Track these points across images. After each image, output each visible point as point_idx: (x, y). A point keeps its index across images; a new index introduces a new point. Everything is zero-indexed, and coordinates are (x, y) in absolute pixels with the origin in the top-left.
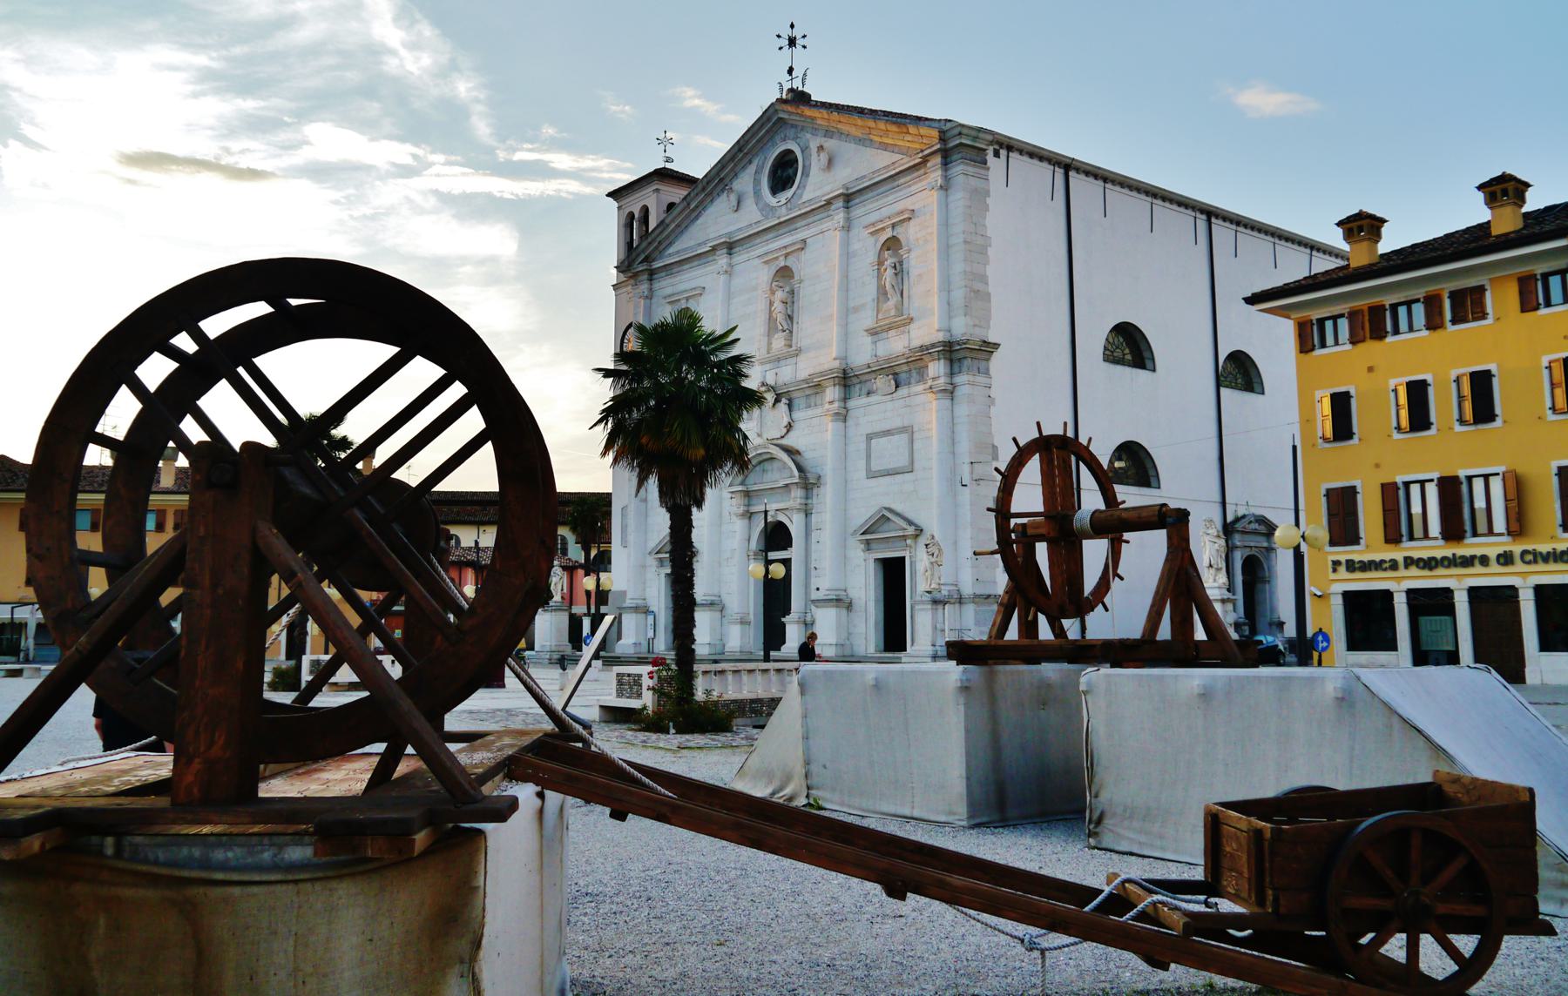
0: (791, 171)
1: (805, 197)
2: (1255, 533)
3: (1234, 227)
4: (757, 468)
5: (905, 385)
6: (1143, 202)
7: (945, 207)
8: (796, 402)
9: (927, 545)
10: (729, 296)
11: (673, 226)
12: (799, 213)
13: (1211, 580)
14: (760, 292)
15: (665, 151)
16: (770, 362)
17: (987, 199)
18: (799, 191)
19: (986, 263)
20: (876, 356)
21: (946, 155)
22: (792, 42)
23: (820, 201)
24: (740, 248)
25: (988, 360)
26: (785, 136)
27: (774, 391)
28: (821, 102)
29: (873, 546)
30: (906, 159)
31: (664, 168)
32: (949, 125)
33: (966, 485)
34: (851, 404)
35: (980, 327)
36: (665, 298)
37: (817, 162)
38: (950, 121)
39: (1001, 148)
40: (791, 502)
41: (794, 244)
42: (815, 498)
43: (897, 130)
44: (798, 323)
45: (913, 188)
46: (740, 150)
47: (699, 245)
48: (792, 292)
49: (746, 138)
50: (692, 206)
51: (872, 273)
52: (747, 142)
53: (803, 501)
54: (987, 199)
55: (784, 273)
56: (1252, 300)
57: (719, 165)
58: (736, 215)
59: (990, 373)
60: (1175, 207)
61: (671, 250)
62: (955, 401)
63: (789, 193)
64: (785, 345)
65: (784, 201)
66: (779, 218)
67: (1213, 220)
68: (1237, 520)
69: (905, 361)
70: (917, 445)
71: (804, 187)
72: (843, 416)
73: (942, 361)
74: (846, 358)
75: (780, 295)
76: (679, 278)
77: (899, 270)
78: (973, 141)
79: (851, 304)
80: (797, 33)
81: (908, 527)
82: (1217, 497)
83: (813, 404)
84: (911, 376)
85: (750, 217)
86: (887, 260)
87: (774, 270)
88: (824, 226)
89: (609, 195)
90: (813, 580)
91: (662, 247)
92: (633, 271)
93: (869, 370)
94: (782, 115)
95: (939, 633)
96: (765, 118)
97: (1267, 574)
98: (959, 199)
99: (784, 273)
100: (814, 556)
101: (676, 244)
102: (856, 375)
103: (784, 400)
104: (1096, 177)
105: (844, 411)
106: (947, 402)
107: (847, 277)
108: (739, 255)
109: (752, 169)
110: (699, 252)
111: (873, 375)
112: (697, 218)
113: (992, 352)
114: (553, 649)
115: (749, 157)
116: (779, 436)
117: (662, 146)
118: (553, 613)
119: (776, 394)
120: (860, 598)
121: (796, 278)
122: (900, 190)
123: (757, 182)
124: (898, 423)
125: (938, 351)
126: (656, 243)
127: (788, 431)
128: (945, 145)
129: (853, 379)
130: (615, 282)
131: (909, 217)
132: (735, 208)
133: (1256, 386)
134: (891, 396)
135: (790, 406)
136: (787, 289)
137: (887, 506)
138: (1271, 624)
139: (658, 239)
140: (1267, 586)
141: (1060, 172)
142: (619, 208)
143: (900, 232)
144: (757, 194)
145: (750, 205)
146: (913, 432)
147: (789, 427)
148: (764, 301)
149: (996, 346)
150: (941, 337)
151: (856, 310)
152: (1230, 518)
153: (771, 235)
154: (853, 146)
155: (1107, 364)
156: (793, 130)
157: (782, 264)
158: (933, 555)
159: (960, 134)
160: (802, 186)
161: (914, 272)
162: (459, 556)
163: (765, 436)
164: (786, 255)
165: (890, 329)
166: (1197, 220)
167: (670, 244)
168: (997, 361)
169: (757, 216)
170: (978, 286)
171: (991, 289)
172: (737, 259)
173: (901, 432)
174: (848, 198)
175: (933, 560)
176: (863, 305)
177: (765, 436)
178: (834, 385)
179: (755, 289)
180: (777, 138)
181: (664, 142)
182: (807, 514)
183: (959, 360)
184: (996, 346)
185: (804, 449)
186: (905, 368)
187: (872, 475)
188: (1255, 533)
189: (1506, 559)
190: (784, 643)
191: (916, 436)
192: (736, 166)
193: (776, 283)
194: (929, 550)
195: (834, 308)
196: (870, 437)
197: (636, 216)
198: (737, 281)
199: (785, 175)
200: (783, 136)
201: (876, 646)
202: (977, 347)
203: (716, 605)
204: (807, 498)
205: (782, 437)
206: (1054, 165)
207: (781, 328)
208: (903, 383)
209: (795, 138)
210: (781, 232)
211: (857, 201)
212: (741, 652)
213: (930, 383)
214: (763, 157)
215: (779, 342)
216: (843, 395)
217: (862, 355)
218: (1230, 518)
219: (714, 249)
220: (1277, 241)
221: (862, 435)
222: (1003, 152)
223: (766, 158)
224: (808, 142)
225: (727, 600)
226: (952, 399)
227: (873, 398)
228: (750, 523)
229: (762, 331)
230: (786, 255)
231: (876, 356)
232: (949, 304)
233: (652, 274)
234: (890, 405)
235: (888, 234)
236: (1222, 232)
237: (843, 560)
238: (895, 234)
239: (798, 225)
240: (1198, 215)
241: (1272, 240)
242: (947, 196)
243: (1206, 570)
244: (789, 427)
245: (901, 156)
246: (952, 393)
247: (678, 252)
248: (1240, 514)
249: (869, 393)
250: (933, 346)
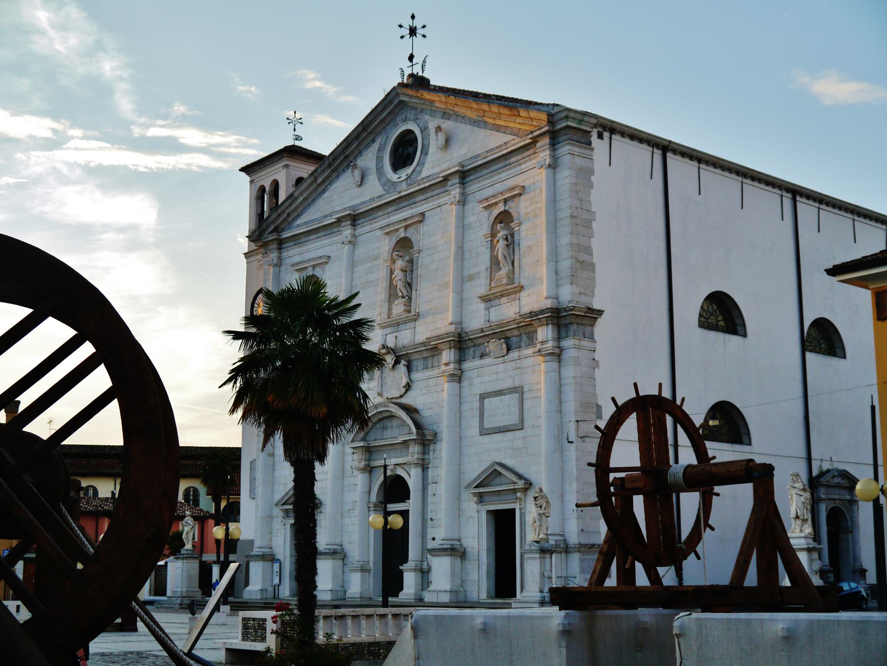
1: (424, 174)
2: (838, 486)
3: (817, 205)
4: (378, 426)
5: (516, 348)
6: (732, 182)
7: (553, 184)
8: (414, 363)
9: (535, 498)
10: (353, 264)
11: (301, 199)
12: (418, 188)
13: (798, 530)
14: (382, 261)
15: (295, 130)
16: (390, 326)
17: (592, 177)
18: (418, 168)
19: (591, 236)
20: (489, 321)
21: (555, 136)
22: (413, 31)
23: (439, 177)
24: (364, 220)
25: (593, 325)
26: (406, 117)
27: (394, 353)
28: (439, 87)
29: (486, 498)
30: (518, 140)
31: (294, 146)
32: (556, 109)
33: (572, 442)
34: (466, 365)
35: (585, 295)
36: (293, 265)
37: (435, 142)
38: (557, 105)
39: (605, 130)
40: (410, 457)
41: (413, 216)
42: (431, 453)
43: (509, 113)
44: (416, 290)
45: (523, 166)
46: (364, 130)
47: (326, 217)
48: (411, 262)
49: (370, 119)
50: (318, 183)
51: (484, 243)
52: (371, 123)
53: (421, 456)
54: (592, 177)
55: (404, 245)
56: (833, 272)
57: (345, 143)
58: (360, 189)
59: (596, 337)
60: (763, 186)
61: (299, 222)
62: (562, 364)
63: (409, 170)
64: (404, 310)
65: (404, 177)
66: (399, 192)
67: (798, 198)
68: (822, 474)
69: (516, 326)
70: (527, 404)
71: (423, 164)
72: (457, 377)
73: (550, 327)
74: (461, 323)
75: (400, 263)
76: (305, 248)
77: (511, 242)
78: (578, 123)
79: (466, 273)
80: (418, 23)
81: (518, 481)
82: (802, 453)
83: (430, 366)
84: (521, 341)
85: (373, 191)
86: (499, 232)
87: (394, 240)
88: (442, 201)
89: (242, 170)
90: (430, 530)
91: (290, 219)
92: (263, 241)
93: (483, 334)
94: (403, 98)
95: (546, 580)
96: (387, 101)
97: (850, 525)
98: (566, 177)
99: (404, 245)
100: (430, 508)
101: (304, 216)
102: (471, 339)
103: (403, 362)
104: (691, 158)
105: (458, 373)
106: (555, 365)
107: (462, 248)
108: (363, 227)
109: (375, 146)
110: (325, 223)
111: (487, 339)
112: (324, 191)
113: (597, 318)
114: (184, 594)
115: (372, 136)
116: (398, 396)
117: (292, 125)
118: (185, 561)
119: (396, 356)
120: (473, 548)
121: (415, 248)
122: (512, 168)
123: (379, 160)
124: (508, 384)
125: (546, 317)
126: (285, 215)
127: (407, 391)
128: (553, 127)
129: (467, 342)
130: (247, 251)
131: (521, 192)
132: (359, 183)
133: (838, 351)
134: (502, 359)
135: (409, 368)
136: (407, 258)
137: (498, 461)
138: (854, 572)
139: (287, 211)
140: (850, 535)
141: (658, 153)
142: (252, 182)
143: (512, 207)
144: (380, 170)
145: (372, 179)
146: (523, 393)
147: (408, 387)
148: (385, 270)
149: (600, 312)
150: (548, 304)
151: (471, 278)
152: (815, 472)
153: (392, 209)
154: (468, 127)
155: (702, 330)
156: (413, 112)
157: (402, 235)
158: (541, 507)
159: (567, 117)
160: (421, 164)
161: (524, 244)
162: (96, 506)
163: (386, 395)
164: (406, 227)
165: (502, 296)
166: (783, 197)
167: (298, 216)
168: (601, 328)
169: (379, 190)
170: (583, 257)
171: (596, 259)
172: (360, 230)
173: (511, 393)
174: (464, 175)
175: (541, 512)
176: (478, 273)
177: (386, 395)
178: (450, 348)
179: (377, 258)
180: (399, 119)
181: (294, 122)
182: (424, 466)
183: (566, 325)
184: (600, 312)
185: (422, 408)
186: (516, 333)
187: (484, 432)
188: (838, 486)
190: (402, 589)
191: (526, 396)
192: (360, 144)
193: (397, 253)
194: (537, 502)
195: (451, 278)
196: (483, 397)
197: (267, 189)
198: (360, 251)
199: (406, 152)
200: (404, 117)
201: (488, 592)
202: (583, 314)
203: (338, 553)
204: (424, 453)
205: (401, 396)
206: (653, 147)
207: (401, 294)
208: (514, 346)
209: (415, 120)
210: (401, 205)
211: (472, 177)
212: (361, 598)
213: (539, 346)
214: (385, 137)
215: (398, 308)
216: (458, 358)
218: (815, 472)
219: (339, 221)
220: (856, 218)
221: (475, 395)
222: (606, 135)
223: (388, 138)
224: (427, 123)
225: (347, 547)
226: (559, 362)
227: (486, 361)
228: (370, 477)
229: (383, 297)
230: (406, 227)
231: (489, 321)
232: (556, 273)
233: (281, 244)
234: (501, 367)
235: (501, 208)
236: (806, 210)
237: (458, 511)
238: (507, 208)
239: (418, 199)
240: (784, 194)
241: (852, 216)
242: (555, 174)
243: (793, 521)
244: (408, 387)
245: (512, 137)
246: (559, 355)
247: (305, 223)
248: (825, 468)
249: (482, 356)
250: (542, 312)
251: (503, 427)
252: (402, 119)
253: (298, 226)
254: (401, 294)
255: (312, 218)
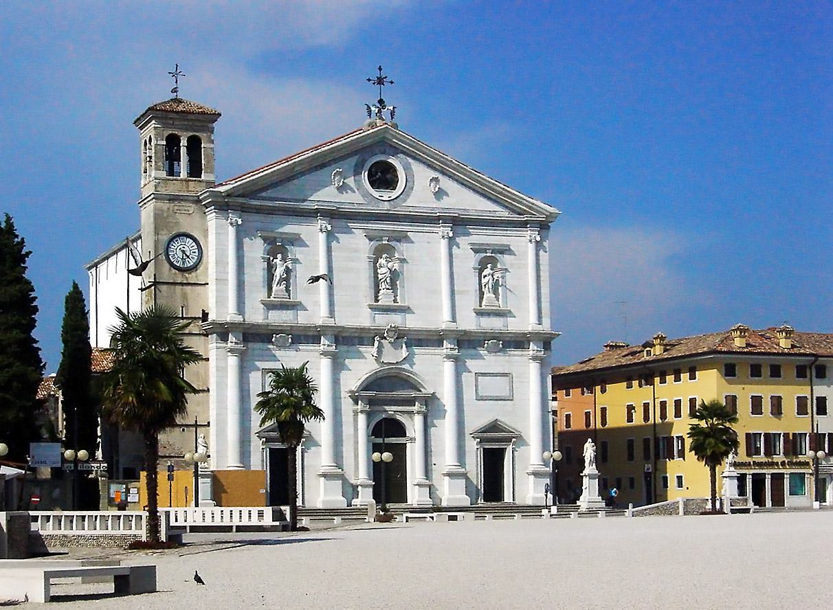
0: (389, 176)
1: (410, 202)
61: (264, 194)
63: (394, 194)
101: (270, 191)
151: (461, 292)
179: (356, 251)
189: (783, 463)
214: (362, 157)
217: (469, 322)
251: (497, 396)
252: (380, 150)
253: (264, 199)
254: (387, 287)
255: (280, 195)
